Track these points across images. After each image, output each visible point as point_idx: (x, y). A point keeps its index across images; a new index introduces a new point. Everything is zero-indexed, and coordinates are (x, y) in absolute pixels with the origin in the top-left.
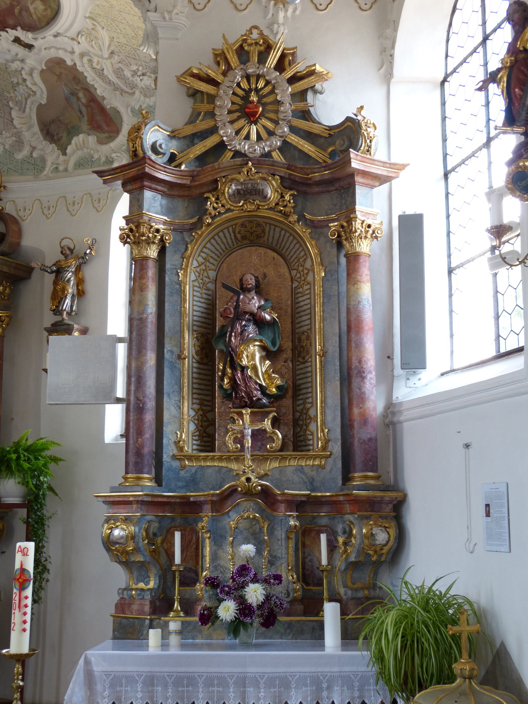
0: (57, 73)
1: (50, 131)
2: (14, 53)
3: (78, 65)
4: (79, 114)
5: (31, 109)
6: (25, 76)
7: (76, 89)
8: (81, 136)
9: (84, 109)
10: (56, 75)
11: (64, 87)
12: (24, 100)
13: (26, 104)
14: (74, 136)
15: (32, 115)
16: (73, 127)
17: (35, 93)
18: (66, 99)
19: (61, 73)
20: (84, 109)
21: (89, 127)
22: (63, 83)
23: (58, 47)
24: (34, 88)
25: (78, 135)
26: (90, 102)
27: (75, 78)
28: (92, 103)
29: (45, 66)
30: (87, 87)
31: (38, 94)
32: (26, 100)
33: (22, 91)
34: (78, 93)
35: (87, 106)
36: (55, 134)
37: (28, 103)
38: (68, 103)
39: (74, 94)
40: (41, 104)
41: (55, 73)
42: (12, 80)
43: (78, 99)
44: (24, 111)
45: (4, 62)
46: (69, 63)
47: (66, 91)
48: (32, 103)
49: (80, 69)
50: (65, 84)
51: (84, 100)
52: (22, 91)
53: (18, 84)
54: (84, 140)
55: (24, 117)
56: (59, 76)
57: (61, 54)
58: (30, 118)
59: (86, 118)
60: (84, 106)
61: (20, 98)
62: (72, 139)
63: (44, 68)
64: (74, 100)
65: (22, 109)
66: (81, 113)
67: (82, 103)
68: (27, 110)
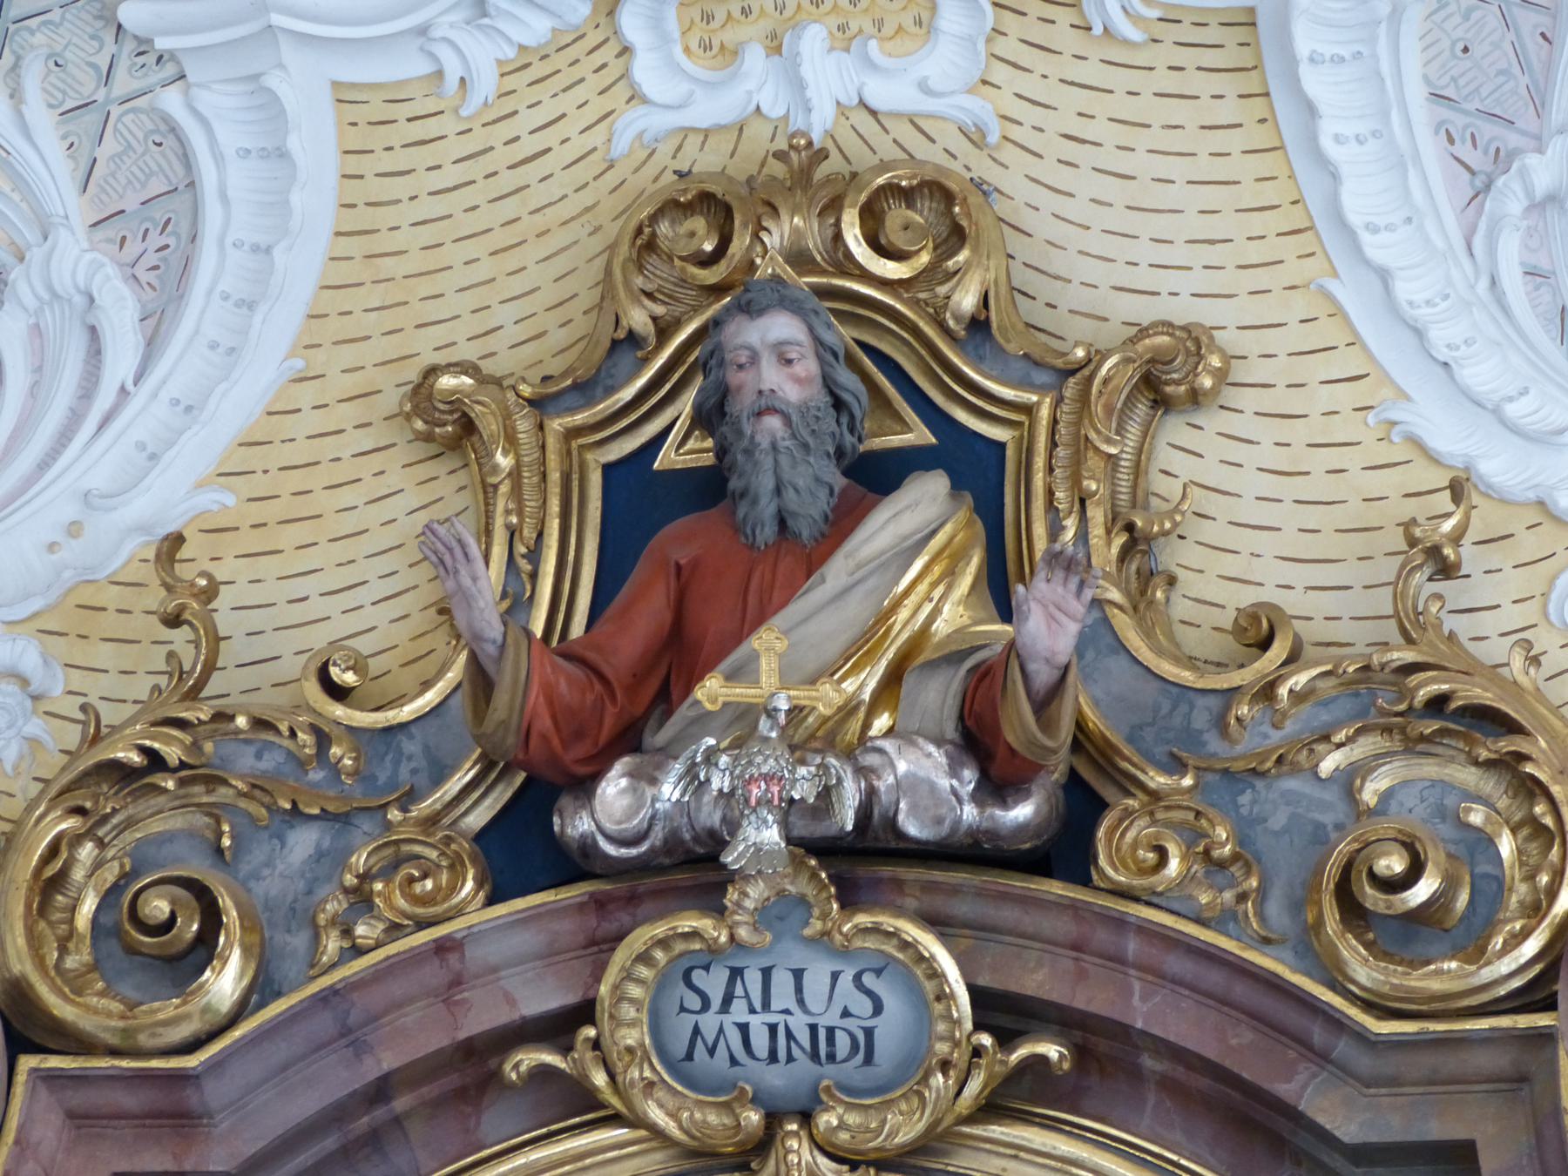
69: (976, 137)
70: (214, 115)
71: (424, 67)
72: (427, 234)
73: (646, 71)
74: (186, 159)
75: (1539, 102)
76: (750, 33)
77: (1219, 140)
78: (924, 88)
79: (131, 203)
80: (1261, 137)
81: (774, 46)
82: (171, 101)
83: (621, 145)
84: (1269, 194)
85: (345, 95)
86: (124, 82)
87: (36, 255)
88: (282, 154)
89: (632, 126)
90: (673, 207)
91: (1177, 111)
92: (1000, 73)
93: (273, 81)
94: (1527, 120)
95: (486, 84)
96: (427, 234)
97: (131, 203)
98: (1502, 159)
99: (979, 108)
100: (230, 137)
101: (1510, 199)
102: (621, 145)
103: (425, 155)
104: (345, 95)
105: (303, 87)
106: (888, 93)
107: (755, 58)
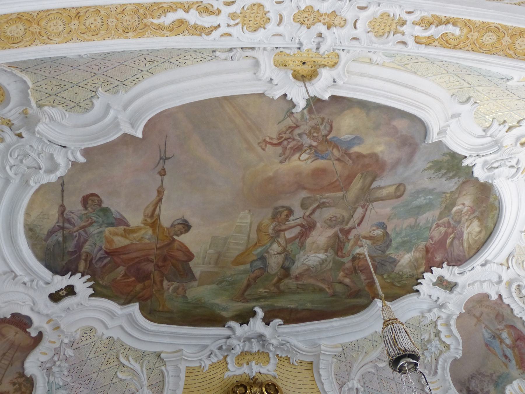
0: (478, 314)
1: (471, 389)
2: (435, 298)
3: (504, 296)
4: (504, 359)
5: (444, 369)
6: (440, 328)
7: (498, 329)
8: (515, 383)
9: (509, 352)
10: (477, 318)
11: (484, 330)
12: (434, 360)
13: (437, 363)
14: (505, 386)
15: (445, 375)
16: (499, 377)
17: (448, 347)
18: (487, 345)
19: (482, 314)
20: (509, 352)
21: (521, 371)
22: (483, 326)
23: (482, 280)
24: (448, 341)
25: (511, 382)
26: (516, 341)
27: (497, 315)
28: (518, 342)
29: (464, 309)
30: (512, 324)
31: (452, 347)
32: (437, 360)
33: (433, 349)
34: (501, 334)
35: (513, 347)
36: (478, 390)
37: (440, 362)
38: (489, 349)
39: (496, 336)
40: (455, 360)
41: (474, 315)
42: (422, 337)
43: (502, 341)
44: (436, 373)
45: (419, 314)
46: (494, 297)
47: (487, 336)
48: (445, 361)
49: (506, 301)
50: (486, 327)
51: (508, 341)
52: (433, 349)
53: (429, 341)
54: (520, 387)
55: (436, 381)
56: (479, 319)
57: (486, 289)
58: (445, 380)
59: (514, 362)
60: (510, 348)
61: (430, 359)
62: (504, 389)
63: (464, 311)
64: (496, 343)
65: (432, 372)
66: (506, 357)
67: (507, 345)
68: (439, 371)
69: (275, 378)
70: (169, 371)
71: (198, 365)
72: (197, 389)
73: (230, 367)
74: (163, 377)
75: (349, 375)
76: (244, 362)
77: (306, 379)
78: (268, 370)
79: (154, 383)
80: (312, 379)
81: (248, 364)
82: (163, 368)
83: (226, 377)
84: (313, 387)
85: (187, 368)
86: (157, 365)
87: (141, 391)
88: (178, 376)
89: (227, 374)
90: (238, 386)
91: (300, 375)
92: (278, 369)
93: (179, 366)
94: (347, 378)
95: (207, 368)
96: (197, 389)
97: (154, 383)
98: (344, 383)
99: (275, 373)
100: (171, 374)
101: (345, 388)
102: (226, 377)
103: (197, 377)
104: (187, 368)
105: (183, 367)
106: (263, 371)
107: (245, 365)
